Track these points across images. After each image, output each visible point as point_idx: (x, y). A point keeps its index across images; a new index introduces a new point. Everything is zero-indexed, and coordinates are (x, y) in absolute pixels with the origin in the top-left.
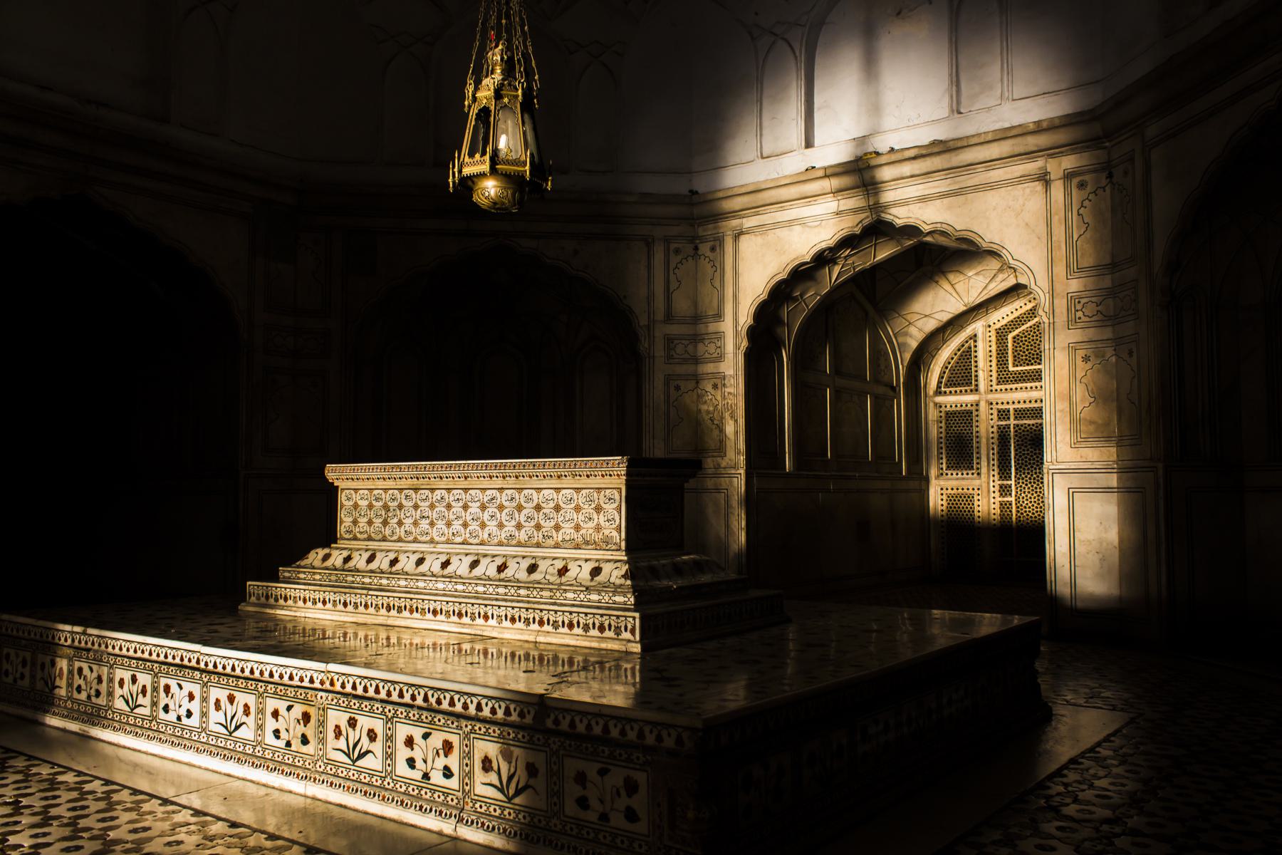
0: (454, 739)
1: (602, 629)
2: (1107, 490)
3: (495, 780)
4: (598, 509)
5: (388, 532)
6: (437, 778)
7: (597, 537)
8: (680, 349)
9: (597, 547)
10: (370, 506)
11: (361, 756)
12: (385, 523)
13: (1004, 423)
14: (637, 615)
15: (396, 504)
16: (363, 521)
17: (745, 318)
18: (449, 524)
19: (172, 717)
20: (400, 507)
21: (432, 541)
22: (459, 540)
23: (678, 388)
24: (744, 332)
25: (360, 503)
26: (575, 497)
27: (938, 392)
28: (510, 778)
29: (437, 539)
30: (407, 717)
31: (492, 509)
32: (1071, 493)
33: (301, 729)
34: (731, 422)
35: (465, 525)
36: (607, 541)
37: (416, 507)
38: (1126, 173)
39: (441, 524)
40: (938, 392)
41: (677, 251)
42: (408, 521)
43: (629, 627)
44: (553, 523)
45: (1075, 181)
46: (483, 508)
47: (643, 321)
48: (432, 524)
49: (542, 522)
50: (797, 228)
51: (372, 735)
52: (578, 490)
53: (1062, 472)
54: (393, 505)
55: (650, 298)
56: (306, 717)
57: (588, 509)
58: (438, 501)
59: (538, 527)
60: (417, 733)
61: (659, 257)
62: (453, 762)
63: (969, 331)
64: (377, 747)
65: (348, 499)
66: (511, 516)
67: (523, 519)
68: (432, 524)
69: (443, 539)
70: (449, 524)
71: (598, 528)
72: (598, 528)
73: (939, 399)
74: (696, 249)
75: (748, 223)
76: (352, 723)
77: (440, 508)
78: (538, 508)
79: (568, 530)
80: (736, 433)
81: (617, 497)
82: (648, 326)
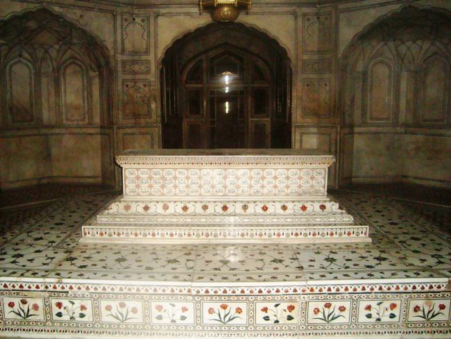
0: (398, 303)
1: (349, 234)
2: (314, 133)
3: (421, 313)
4: (312, 178)
6: (385, 319)
8: (128, 67)
9: (310, 194)
10: (150, 178)
11: (333, 319)
13: (212, 96)
14: (368, 227)
16: (144, 187)
17: (159, 55)
19: (166, 320)
20: (175, 178)
21: (201, 195)
23: (127, 86)
24: (160, 62)
26: (299, 172)
27: (186, 82)
28: (429, 312)
29: (203, 194)
30: (368, 297)
32: (302, 134)
33: (288, 313)
34: (154, 103)
36: (317, 192)
38: (326, 19)
39: (207, 187)
40: (186, 82)
41: (126, 20)
43: (364, 232)
44: (285, 185)
45: (306, 18)
47: (112, 53)
48: (200, 187)
49: (278, 185)
50: (188, 17)
52: (300, 169)
53: (298, 127)
54: (168, 177)
55: (115, 42)
56: (291, 308)
59: (275, 187)
61: (119, 22)
62: (396, 312)
63: (198, 59)
65: (131, 174)
68: (200, 187)
71: (312, 186)
72: (312, 186)
73: (188, 85)
74: (134, 19)
75: (163, 11)
79: (294, 188)
80: (156, 108)
81: (323, 172)
82: (114, 56)
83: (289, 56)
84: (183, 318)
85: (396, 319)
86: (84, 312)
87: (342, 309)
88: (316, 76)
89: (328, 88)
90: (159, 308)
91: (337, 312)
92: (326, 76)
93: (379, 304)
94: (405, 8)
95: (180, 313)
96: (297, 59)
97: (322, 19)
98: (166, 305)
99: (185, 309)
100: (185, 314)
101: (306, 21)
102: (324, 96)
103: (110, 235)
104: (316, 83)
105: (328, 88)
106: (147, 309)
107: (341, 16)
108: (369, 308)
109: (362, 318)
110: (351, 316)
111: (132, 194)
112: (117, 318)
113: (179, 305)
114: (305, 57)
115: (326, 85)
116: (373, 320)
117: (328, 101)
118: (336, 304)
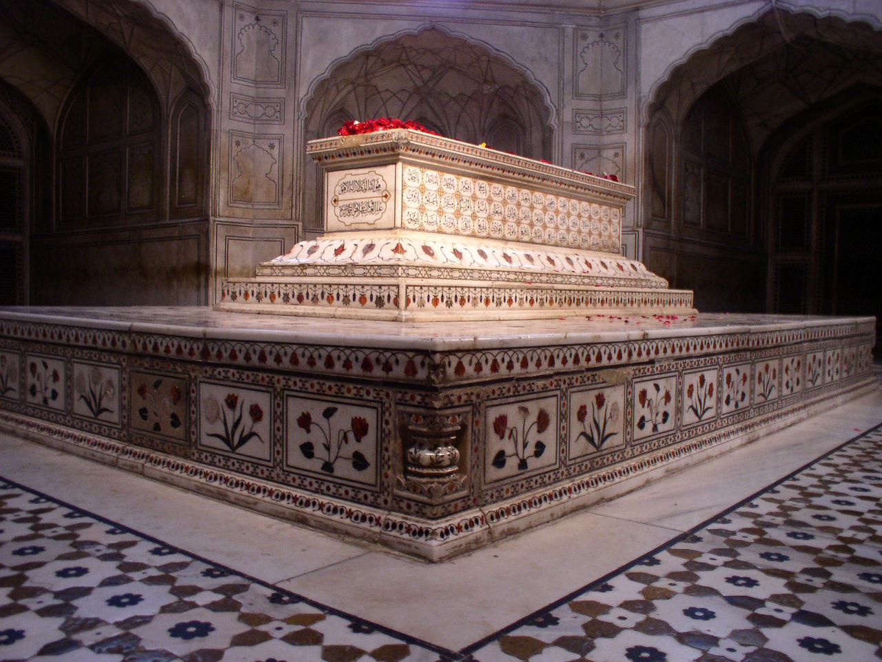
4: (610, 222)
5: (461, 225)
7: (610, 243)
10: (441, 192)
12: (458, 214)
15: (469, 194)
16: (431, 209)
18: (518, 223)
20: (474, 198)
22: (526, 238)
25: (428, 186)
31: (551, 213)
35: (532, 225)
37: (490, 200)
42: (482, 215)
44: (588, 230)
46: (545, 210)
49: (582, 228)
57: (605, 221)
58: (510, 198)
59: (579, 232)
65: (413, 179)
66: (563, 219)
67: (571, 224)
68: (504, 221)
69: (513, 237)
70: (518, 223)
71: (610, 237)
72: (610, 237)
77: (512, 206)
78: (579, 216)
83: (207, 79)
88: (249, 128)
89: (276, 152)
92: (275, 129)
94: (426, 30)
96: (220, 87)
97: (266, 22)
101: (237, 20)
102: (266, 168)
103: (449, 304)
104: (251, 142)
105: (276, 152)
107: (306, 24)
111: (411, 226)
114: (236, 87)
115: (272, 146)
117: (275, 174)
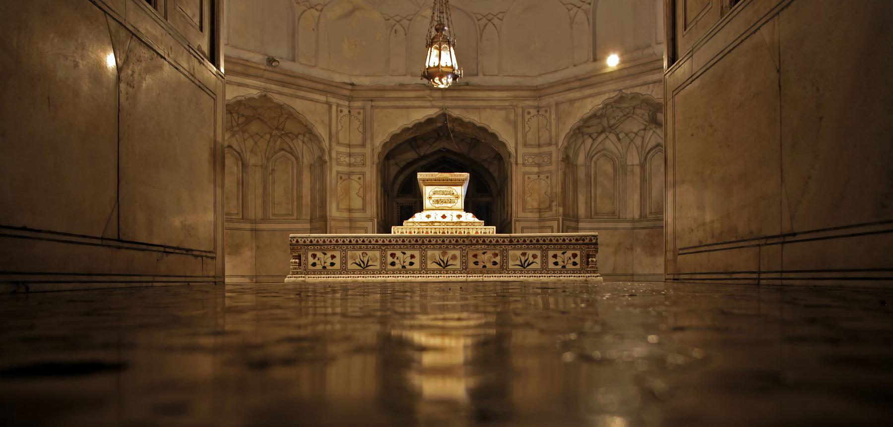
0: (578, 252)
11: (529, 265)
51: (534, 256)
60: (559, 253)
62: (577, 260)
64: (538, 260)
76: (524, 254)
84: (411, 264)
85: (578, 267)
86: (334, 261)
87: (534, 256)
90: (393, 255)
91: (531, 259)
93: (563, 253)
95: (408, 260)
98: (398, 253)
99: (412, 257)
100: (413, 260)
106: (383, 257)
108: (555, 256)
109: (551, 266)
110: (542, 263)
112: (360, 265)
113: (409, 253)
116: (559, 267)
118: (530, 253)
